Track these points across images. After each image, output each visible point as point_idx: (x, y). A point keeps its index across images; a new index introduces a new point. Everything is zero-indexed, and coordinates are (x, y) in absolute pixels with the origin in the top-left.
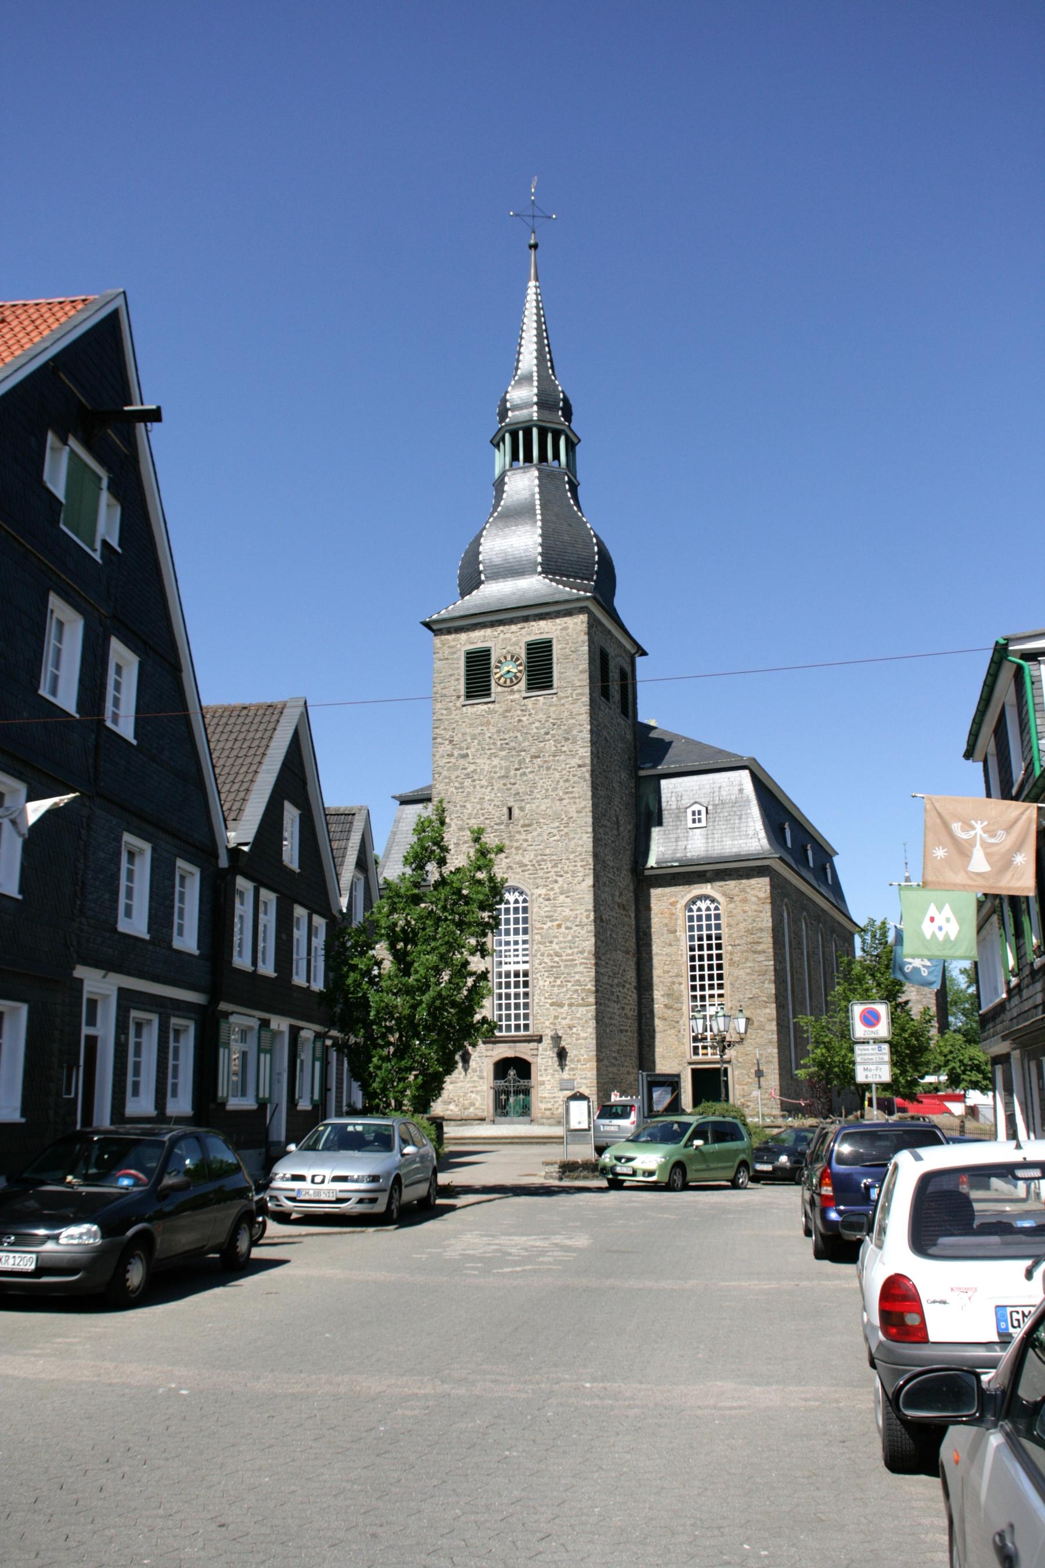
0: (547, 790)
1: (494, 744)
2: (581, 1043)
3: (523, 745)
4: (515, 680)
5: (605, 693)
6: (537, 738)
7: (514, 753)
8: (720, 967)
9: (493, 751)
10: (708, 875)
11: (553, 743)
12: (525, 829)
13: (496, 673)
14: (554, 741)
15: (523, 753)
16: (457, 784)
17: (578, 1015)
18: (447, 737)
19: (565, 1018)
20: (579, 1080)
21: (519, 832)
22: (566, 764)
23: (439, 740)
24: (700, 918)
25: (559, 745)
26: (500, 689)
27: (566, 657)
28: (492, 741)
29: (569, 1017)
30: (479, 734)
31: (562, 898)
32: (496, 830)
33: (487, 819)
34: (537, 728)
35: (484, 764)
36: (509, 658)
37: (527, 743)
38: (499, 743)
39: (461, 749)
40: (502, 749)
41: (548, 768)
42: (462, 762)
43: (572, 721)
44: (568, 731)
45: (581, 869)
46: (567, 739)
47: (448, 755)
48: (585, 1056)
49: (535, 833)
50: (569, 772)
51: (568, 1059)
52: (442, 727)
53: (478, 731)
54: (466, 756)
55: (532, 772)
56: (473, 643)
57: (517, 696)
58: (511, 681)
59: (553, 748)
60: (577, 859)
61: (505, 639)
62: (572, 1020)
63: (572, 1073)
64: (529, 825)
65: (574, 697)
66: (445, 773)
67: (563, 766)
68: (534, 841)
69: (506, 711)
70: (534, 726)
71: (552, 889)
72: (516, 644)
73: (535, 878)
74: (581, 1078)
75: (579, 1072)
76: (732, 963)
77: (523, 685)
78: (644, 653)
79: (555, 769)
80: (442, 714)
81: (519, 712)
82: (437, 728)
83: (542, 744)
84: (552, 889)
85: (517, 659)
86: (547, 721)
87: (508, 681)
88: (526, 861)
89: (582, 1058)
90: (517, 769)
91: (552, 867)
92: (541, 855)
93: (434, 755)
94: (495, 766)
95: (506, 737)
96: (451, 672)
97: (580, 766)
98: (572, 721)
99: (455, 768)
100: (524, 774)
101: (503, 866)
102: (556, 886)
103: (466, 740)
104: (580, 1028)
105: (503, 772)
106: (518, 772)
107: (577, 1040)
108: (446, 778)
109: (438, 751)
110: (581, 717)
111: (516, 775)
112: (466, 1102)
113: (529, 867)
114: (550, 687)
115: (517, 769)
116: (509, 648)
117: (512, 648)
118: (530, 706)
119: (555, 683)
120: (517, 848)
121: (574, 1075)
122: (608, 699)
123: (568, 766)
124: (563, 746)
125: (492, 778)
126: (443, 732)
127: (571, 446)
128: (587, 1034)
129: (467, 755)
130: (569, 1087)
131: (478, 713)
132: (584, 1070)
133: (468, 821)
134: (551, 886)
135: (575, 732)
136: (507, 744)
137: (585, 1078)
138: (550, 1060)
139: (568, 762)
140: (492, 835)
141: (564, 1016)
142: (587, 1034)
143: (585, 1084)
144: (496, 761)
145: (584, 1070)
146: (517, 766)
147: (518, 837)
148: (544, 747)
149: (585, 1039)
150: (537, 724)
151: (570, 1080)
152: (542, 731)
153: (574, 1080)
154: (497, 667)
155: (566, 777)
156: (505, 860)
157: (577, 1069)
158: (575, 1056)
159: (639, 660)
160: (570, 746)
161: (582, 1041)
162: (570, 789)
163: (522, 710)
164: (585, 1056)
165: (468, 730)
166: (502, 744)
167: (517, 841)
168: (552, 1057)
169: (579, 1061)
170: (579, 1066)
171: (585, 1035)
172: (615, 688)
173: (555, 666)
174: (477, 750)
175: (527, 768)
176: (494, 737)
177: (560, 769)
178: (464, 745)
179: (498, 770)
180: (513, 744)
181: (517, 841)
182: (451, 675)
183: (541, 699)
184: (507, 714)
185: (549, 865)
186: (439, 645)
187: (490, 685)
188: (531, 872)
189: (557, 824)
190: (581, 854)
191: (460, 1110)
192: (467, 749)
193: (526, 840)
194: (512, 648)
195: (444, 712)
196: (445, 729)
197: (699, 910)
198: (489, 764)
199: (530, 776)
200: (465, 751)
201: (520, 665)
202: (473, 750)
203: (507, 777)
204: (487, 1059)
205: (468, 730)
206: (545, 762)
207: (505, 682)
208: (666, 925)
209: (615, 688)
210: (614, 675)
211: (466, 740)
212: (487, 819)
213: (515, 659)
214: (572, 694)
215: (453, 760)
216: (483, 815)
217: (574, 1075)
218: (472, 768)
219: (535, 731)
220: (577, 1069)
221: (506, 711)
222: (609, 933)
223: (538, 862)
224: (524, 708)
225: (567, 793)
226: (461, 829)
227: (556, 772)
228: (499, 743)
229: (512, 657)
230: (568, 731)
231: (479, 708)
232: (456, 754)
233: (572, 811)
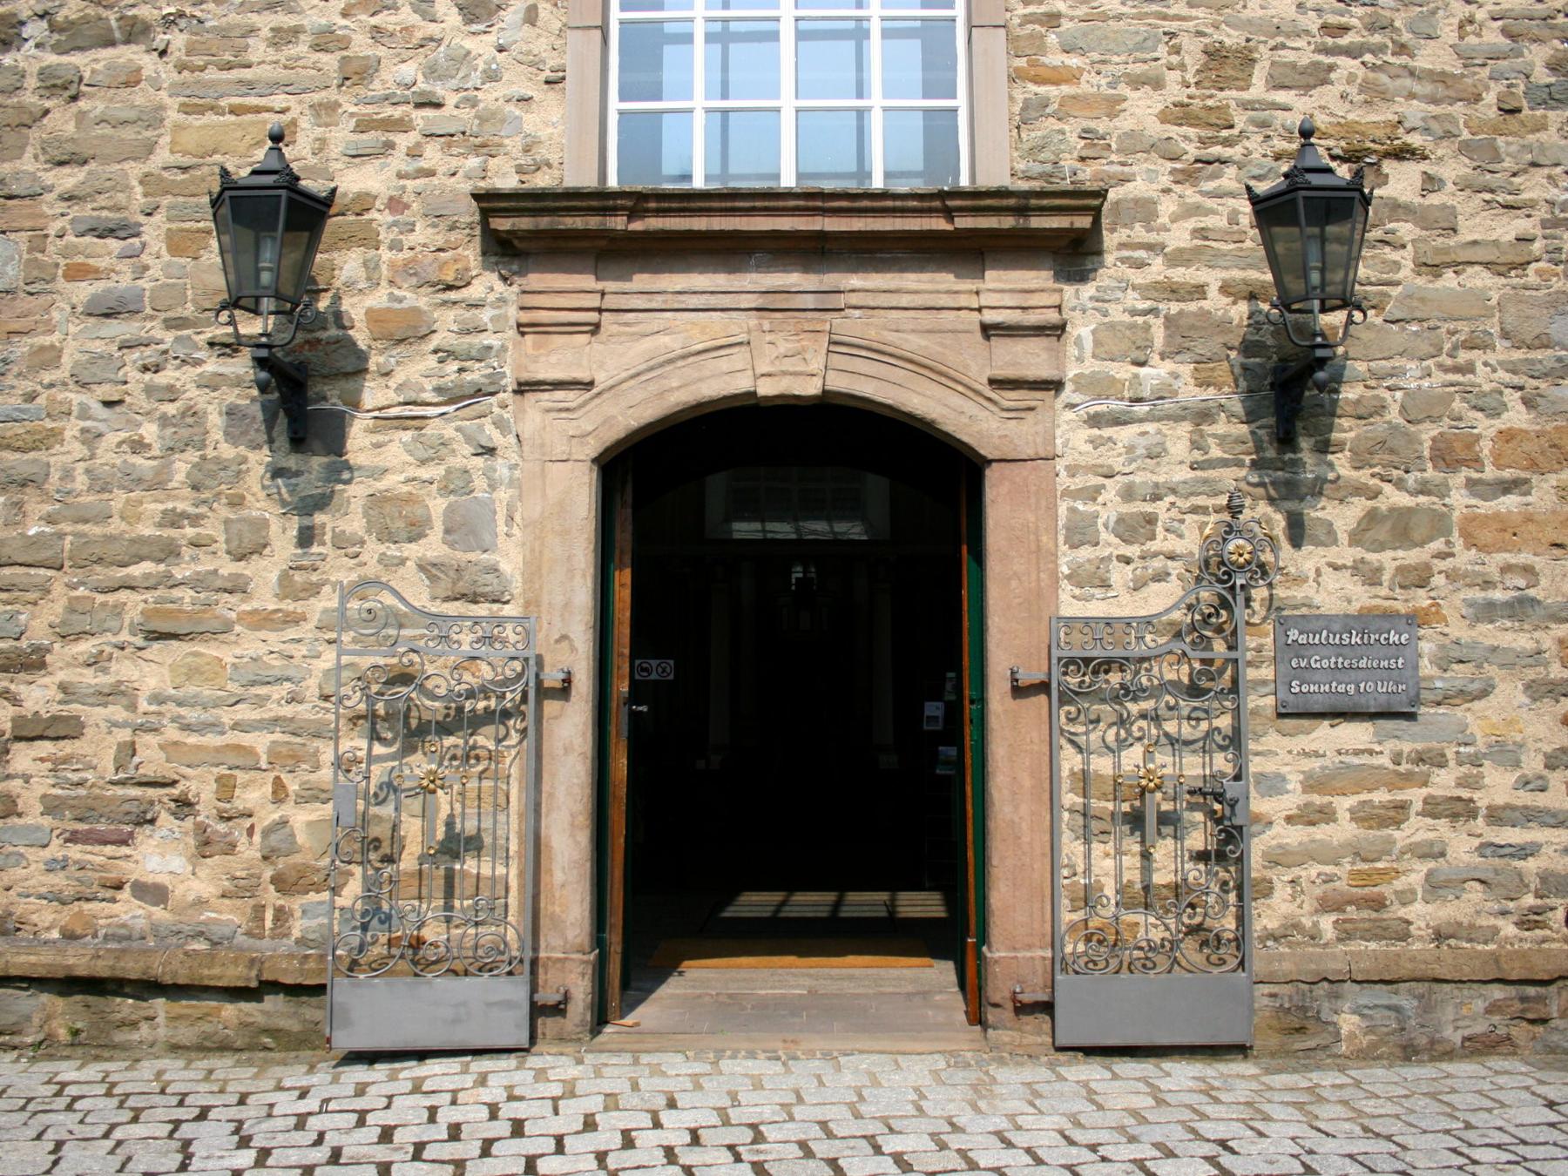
2: (1482, 296)
17: (1430, 57)
19: (1316, 77)
20: (1458, 630)
29: (1346, 64)
48: (1517, 416)
51: (1346, 430)
62: (1374, 94)
63: (1389, 560)
74: (1487, 612)
75: (1464, 558)
89: (1486, 427)
104: (1452, 169)
107: (1431, 268)
112: (302, 818)
121: (1418, 578)
128: (1520, 225)
130: (1378, 692)
132: (1508, 531)
137: (1520, 609)
138: (1178, 438)
141: (1302, 54)
142: (1520, 225)
143: (1512, 661)
145: (1508, 531)
149: (1508, 265)
151: (1365, 621)
153: (1415, 620)
157: (1439, 524)
158: (1420, 409)
161: (1479, 278)
164: (1517, 416)
168: (1203, 416)
169: (1449, 455)
170: (1459, 499)
171: (1507, 228)
191: (240, 889)
204: (534, 414)
217: (1418, 578)
220: (1439, 524)
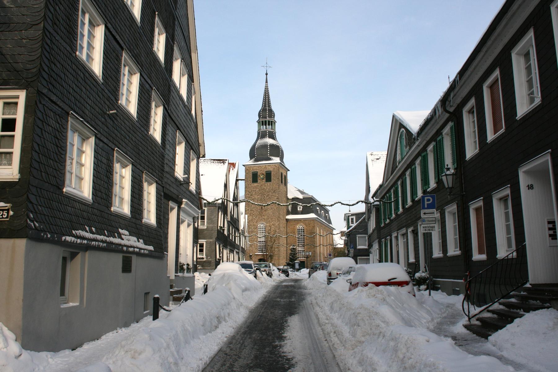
4: (263, 179)
5: (282, 182)
6: (268, 192)
8: (304, 240)
10: (302, 221)
24: (300, 230)
26: (260, 181)
27: (274, 175)
31: (273, 226)
35: (256, 197)
40: (260, 194)
42: (251, 196)
44: (274, 191)
53: (255, 190)
54: (252, 195)
57: (263, 183)
72: (263, 171)
76: (306, 239)
77: (264, 180)
78: (289, 170)
88: (265, 218)
102: (271, 224)
105: (260, 199)
114: (271, 181)
118: (266, 185)
119: (272, 180)
120: (263, 215)
127: (275, 123)
129: (252, 195)
135: (276, 191)
144: (259, 197)
159: (288, 172)
172: (283, 180)
173: (272, 176)
178: (252, 192)
183: (269, 183)
189: (272, 211)
209: (283, 180)
210: (283, 177)
218: (253, 198)
226: (251, 210)
230: (274, 191)
231: (255, 184)
232: (250, 194)
233: (275, 208)
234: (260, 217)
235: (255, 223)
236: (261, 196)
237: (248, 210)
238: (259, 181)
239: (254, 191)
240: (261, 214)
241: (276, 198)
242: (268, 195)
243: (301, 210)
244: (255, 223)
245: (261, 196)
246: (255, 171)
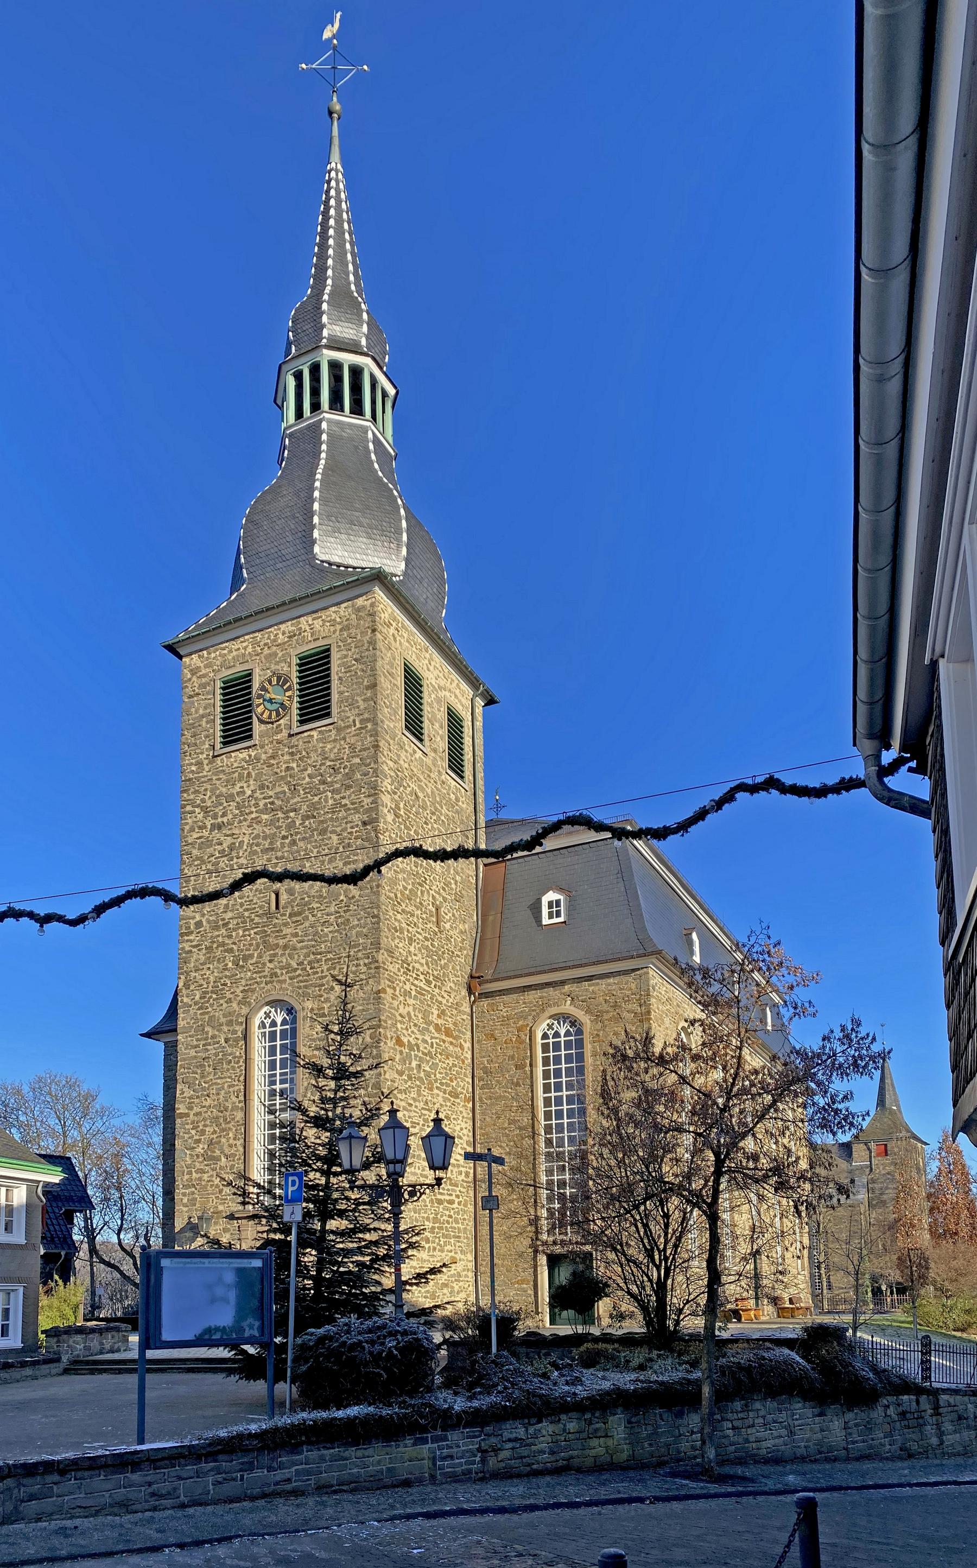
0: (323, 862)
1: (256, 805)
3: (292, 801)
6: (311, 790)
7: (280, 815)
9: (253, 816)
11: (329, 794)
12: (294, 919)
13: (258, 706)
14: (333, 792)
15: (292, 814)
16: (209, 866)
18: (198, 802)
21: (286, 925)
22: (346, 823)
23: (189, 808)
25: (337, 797)
26: (263, 727)
28: (253, 802)
30: (238, 793)
32: (258, 923)
33: (247, 910)
34: (310, 776)
36: (274, 682)
37: (297, 799)
38: (261, 803)
39: (215, 817)
40: (265, 811)
41: (323, 832)
43: (357, 760)
45: (364, 969)
46: (348, 787)
47: (200, 828)
49: (307, 924)
50: (351, 833)
52: (192, 790)
53: (237, 789)
55: (304, 839)
56: (230, 667)
58: (278, 714)
59: (331, 802)
60: (360, 954)
61: (270, 654)
64: (299, 914)
65: (358, 725)
66: (195, 852)
67: (344, 825)
68: (306, 935)
69: (273, 757)
70: (306, 773)
71: (327, 1000)
73: (306, 987)
79: (333, 832)
80: (192, 772)
81: (287, 757)
82: (185, 791)
83: (316, 799)
84: (327, 1000)
85: (285, 682)
86: (324, 764)
87: (274, 714)
90: (284, 837)
91: (328, 970)
92: (313, 953)
93: (183, 830)
94: (257, 836)
95: (271, 793)
96: (201, 712)
97: (364, 824)
98: (357, 760)
99: (208, 843)
100: (294, 843)
101: (266, 973)
103: (221, 804)
105: (267, 844)
106: (287, 841)
108: (198, 858)
109: (187, 824)
110: (365, 754)
111: (283, 845)
113: (299, 972)
114: (328, 715)
115: (284, 837)
116: (273, 667)
117: (277, 667)
119: (335, 710)
120: (285, 947)
122: (419, 736)
123: (349, 825)
124: (344, 798)
125: (255, 853)
126: (192, 797)
131: (236, 765)
133: (224, 915)
134: (325, 996)
136: (272, 803)
139: (350, 819)
140: (252, 932)
146: (283, 833)
147: (286, 931)
148: (319, 802)
150: (310, 771)
152: (316, 780)
154: (260, 696)
155: (346, 841)
156: (268, 965)
160: (353, 796)
162: (353, 858)
163: (292, 754)
165: (224, 790)
166: (266, 805)
167: (284, 937)
174: (235, 816)
175: (297, 833)
176: (258, 794)
177: (338, 829)
179: (260, 840)
180: (278, 803)
181: (284, 937)
182: (203, 716)
184: (272, 762)
185: (325, 968)
186: (189, 676)
187: (251, 724)
188: (301, 978)
190: (365, 949)
192: (222, 816)
193: (296, 935)
194: (277, 667)
195: (194, 768)
196: (194, 792)
197: (557, 1035)
198: (250, 834)
199: (301, 844)
200: (220, 820)
201: (289, 689)
202: (230, 816)
203: (272, 849)
205: (224, 790)
206: (322, 822)
207: (270, 717)
208: (512, 1057)
211: (221, 804)
212: (247, 910)
213: (282, 680)
214: (354, 721)
215: (206, 833)
216: (242, 904)
219: (307, 779)
221: (273, 757)
222: (414, 1064)
223: (310, 963)
224: (294, 750)
225: (349, 863)
226: (217, 928)
227: (335, 837)
228: (261, 803)
229: (279, 679)
231: (239, 755)
234: (266, 958)
235: (235, 1005)
236: (272, 823)
237: (199, 924)
238: (257, 728)
239: (230, 798)
240: (272, 940)
241: (357, 818)
242: (313, 806)
243: (545, 899)
244: (235, 1005)
245: (272, 823)
246: (239, 668)
